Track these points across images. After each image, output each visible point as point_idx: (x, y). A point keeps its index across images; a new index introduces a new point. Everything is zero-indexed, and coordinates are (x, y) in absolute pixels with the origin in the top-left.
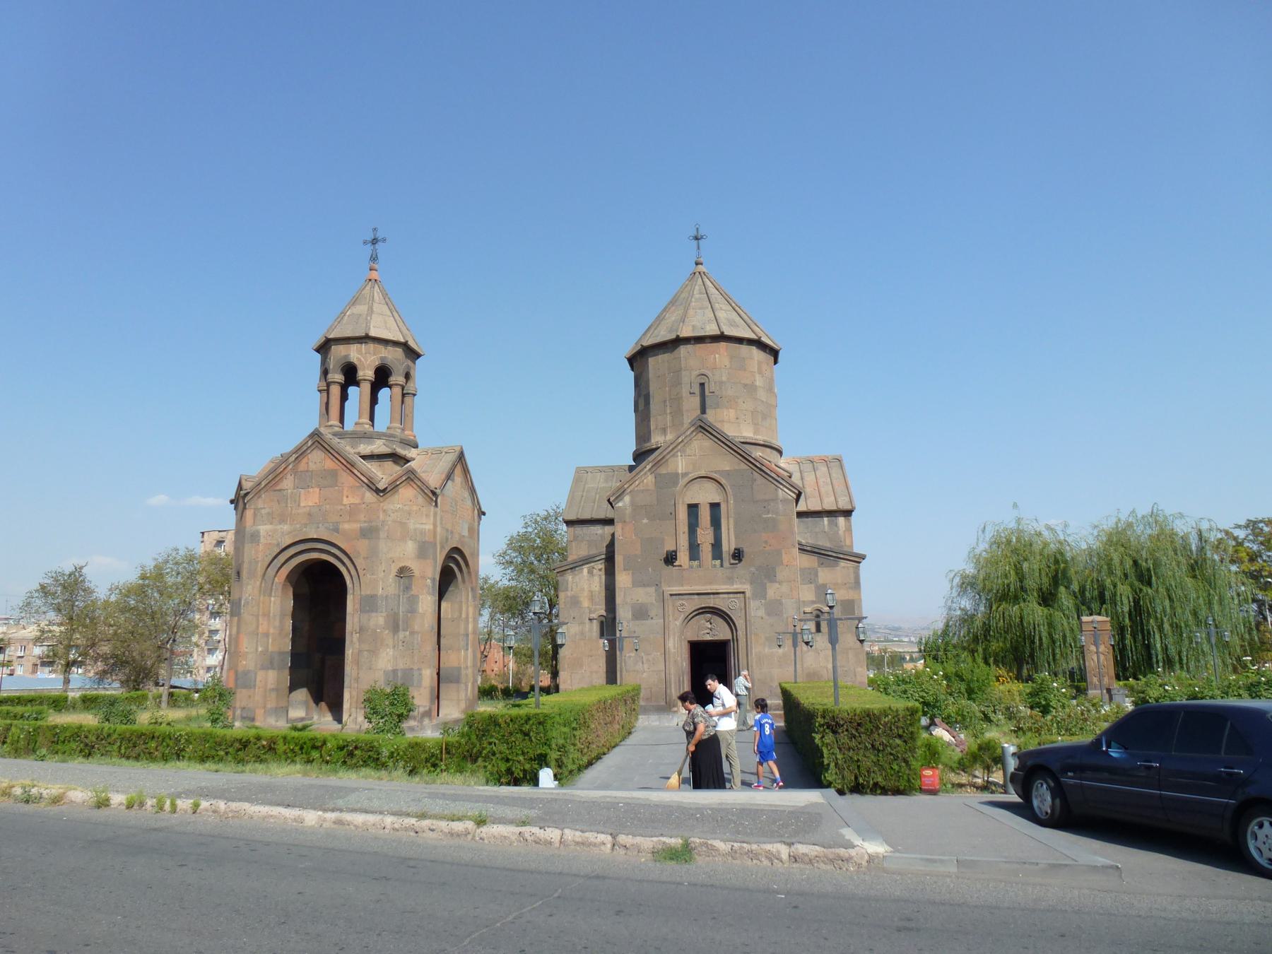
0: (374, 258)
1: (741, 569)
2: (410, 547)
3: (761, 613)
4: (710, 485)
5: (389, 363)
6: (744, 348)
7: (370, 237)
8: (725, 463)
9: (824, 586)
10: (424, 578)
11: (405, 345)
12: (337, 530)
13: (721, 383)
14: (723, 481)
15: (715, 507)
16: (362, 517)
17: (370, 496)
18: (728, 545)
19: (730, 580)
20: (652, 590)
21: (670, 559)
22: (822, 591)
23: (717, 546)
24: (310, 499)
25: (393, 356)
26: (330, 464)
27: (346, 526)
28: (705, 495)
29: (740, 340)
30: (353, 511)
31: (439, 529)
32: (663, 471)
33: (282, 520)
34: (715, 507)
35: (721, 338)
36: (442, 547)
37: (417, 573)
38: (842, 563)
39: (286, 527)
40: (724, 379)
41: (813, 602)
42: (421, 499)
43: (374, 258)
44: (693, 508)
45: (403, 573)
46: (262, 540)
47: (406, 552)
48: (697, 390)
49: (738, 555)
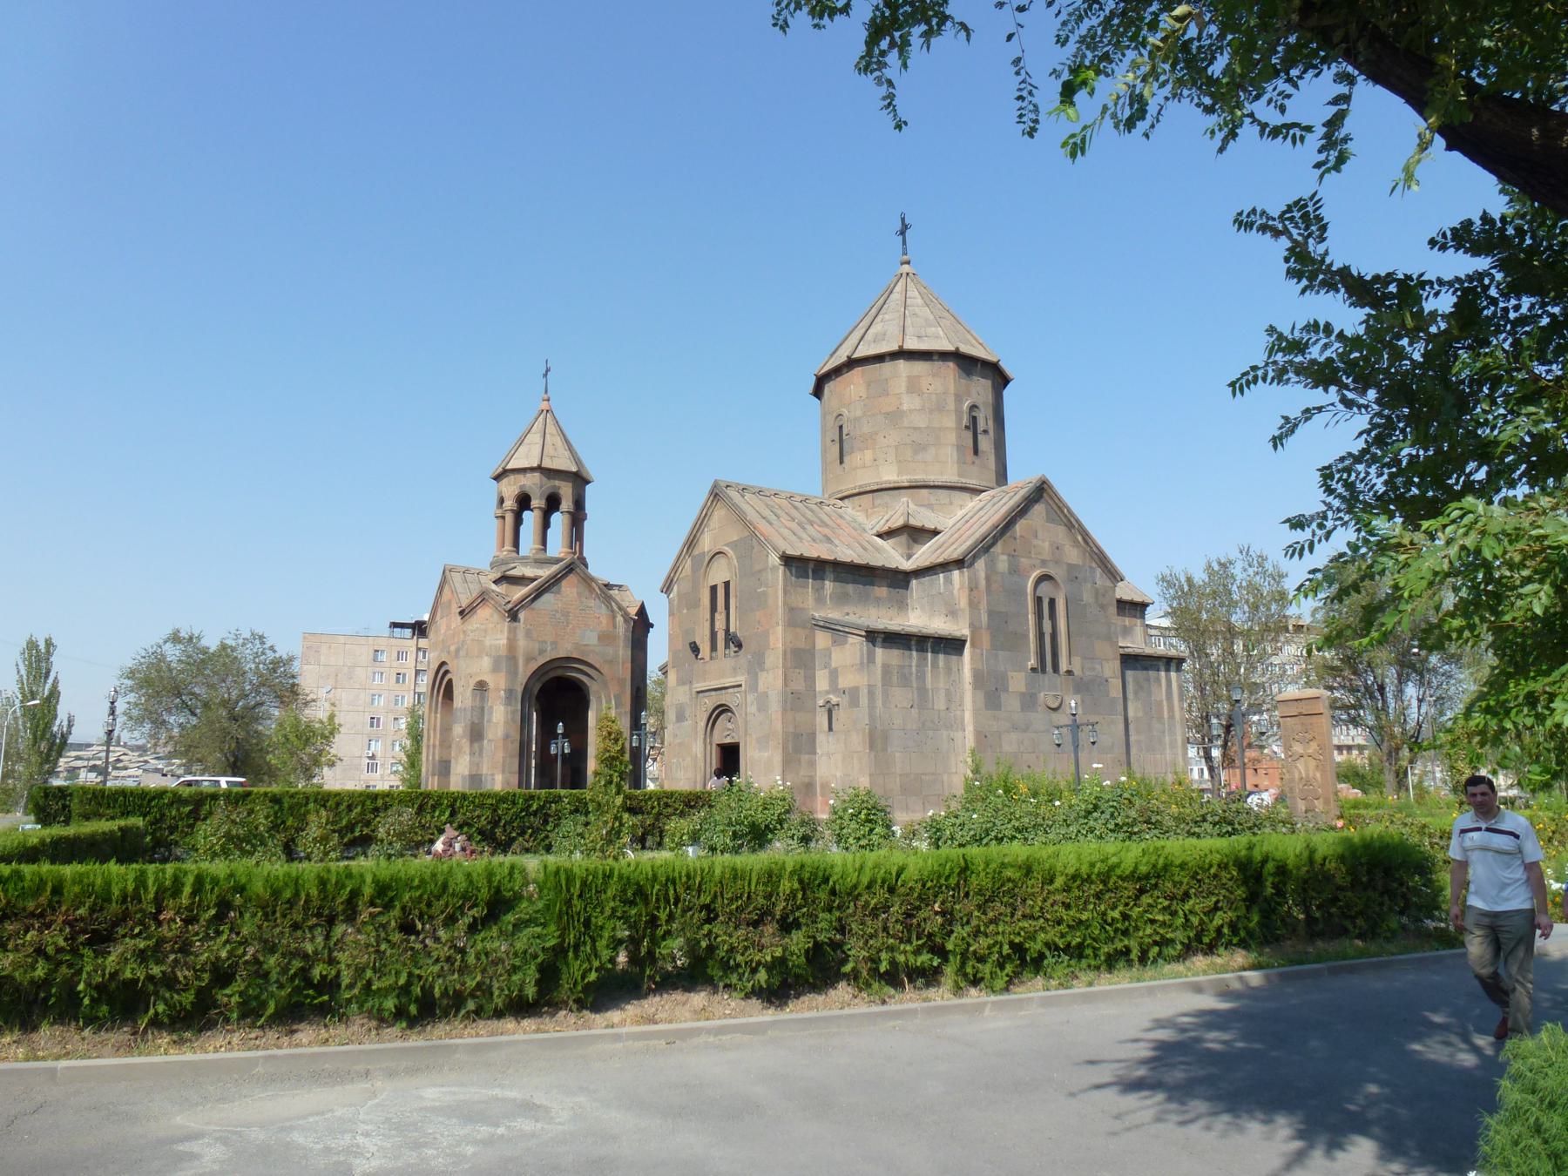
1: (744, 657)
2: (486, 662)
3: (752, 709)
5: (527, 490)
6: (887, 367)
9: (836, 670)
10: (498, 690)
11: (539, 469)
13: (857, 419)
14: (731, 553)
19: (735, 671)
20: (687, 688)
21: (695, 649)
22: (834, 675)
23: (727, 630)
25: (531, 482)
28: (719, 574)
29: (880, 358)
31: (522, 643)
32: (696, 552)
34: (727, 584)
35: (852, 363)
36: (529, 659)
37: (491, 685)
38: (852, 639)
40: (859, 413)
41: (828, 692)
42: (496, 617)
44: (714, 589)
45: (481, 686)
47: (481, 668)
48: (837, 438)
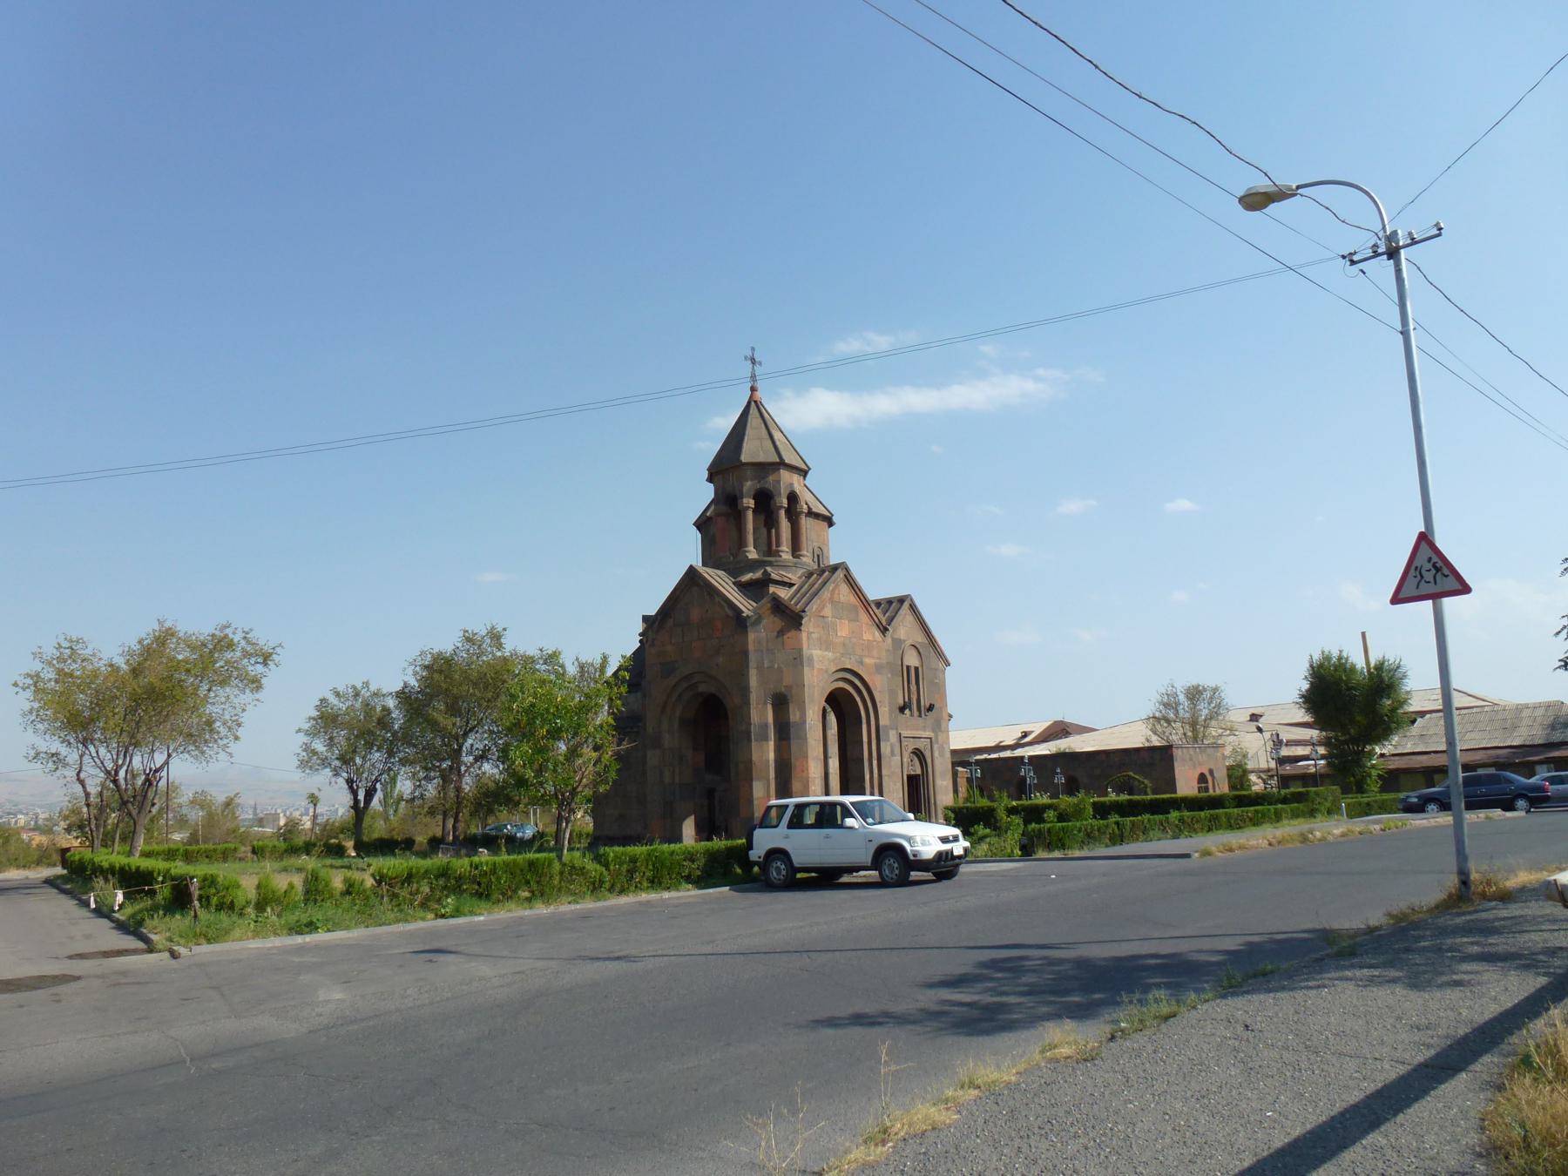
0: (753, 377)
4: (914, 652)
7: (749, 354)
8: (919, 638)
12: (861, 663)
15: (916, 669)
16: (875, 653)
17: (877, 634)
18: (925, 703)
19: (924, 729)
24: (843, 630)
26: (853, 599)
27: (867, 660)
28: (912, 660)
30: (869, 646)
33: (827, 649)
39: (830, 655)
43: (753, 377)
46: (817, 666)
49: (931, 708)
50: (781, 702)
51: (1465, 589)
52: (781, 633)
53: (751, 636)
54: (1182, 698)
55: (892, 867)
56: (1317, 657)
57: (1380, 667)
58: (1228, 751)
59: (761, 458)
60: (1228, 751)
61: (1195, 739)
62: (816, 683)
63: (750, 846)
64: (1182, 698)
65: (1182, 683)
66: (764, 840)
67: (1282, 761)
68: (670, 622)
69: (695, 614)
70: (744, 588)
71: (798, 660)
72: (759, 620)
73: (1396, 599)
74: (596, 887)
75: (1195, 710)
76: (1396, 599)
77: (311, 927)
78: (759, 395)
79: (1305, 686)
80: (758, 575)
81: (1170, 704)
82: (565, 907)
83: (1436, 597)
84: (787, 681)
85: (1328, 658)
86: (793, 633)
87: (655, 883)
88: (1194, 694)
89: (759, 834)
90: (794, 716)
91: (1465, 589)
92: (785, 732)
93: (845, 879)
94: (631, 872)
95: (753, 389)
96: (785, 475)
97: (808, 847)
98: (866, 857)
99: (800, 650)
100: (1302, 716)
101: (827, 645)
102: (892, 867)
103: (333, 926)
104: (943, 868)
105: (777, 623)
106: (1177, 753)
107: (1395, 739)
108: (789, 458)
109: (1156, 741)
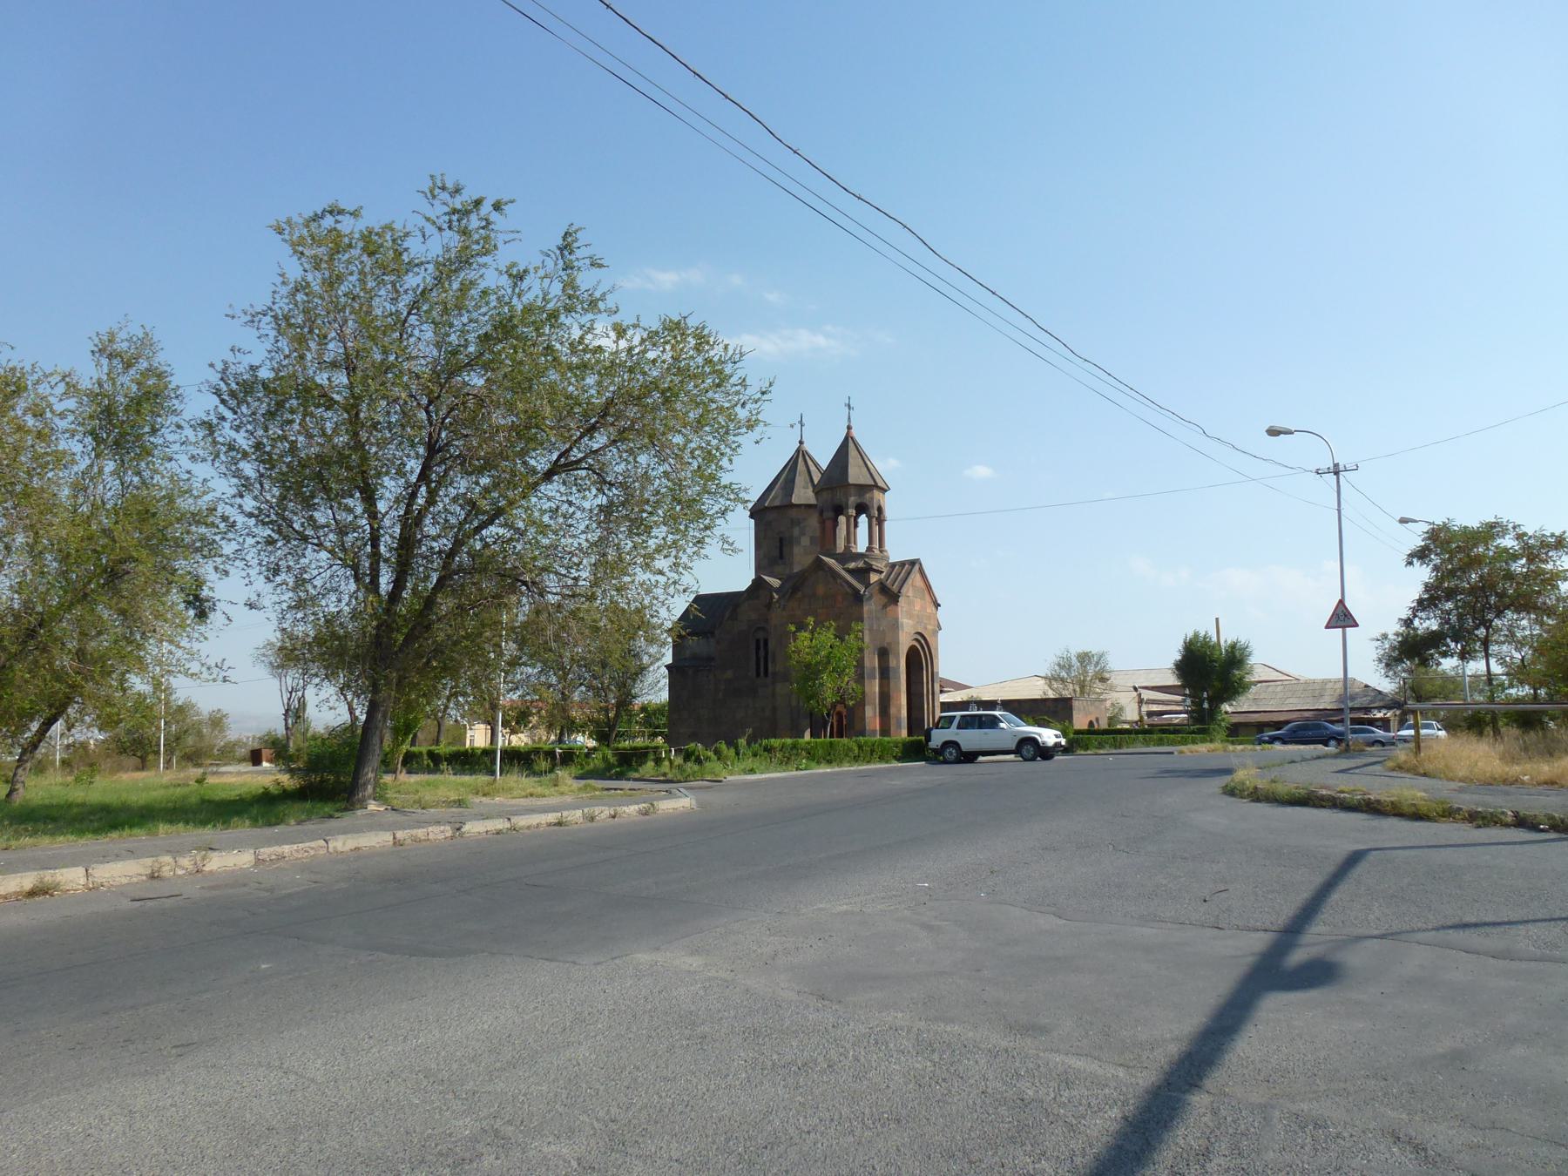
50: (884, 653)
51: (1356, 625)
52: (885, 607)
53: (866, 608)
54: (1074, 660)
55: (1028, 750)
56: (1190, 635)
57: (1233, 646)
58: (1108, 704)
59: (862, 481)
60: (1108, 704)
61: (1082, 692)
62: (905, 642)
63: (928, 739)
64: (1074, 659)
65: (1076, 649)
66: (938, 737)
67: (1150, 714)
68: (799, 594)
69: (821, 590)
70: (849, 571)
71: (895, 626)
72: (871, 597)
73: (1327, 627)
74: (856, 759)
75: (1087, 671)
76: (1327, 627)
77: (752, 771)
78: (854, 433)
79: (1179, 657)
80: (861, 564)
81: (1065, 665)
82: (846, 768)
83: (1344, 627)
84: (888, 640)
85: (1196, 635)
86: (891, 608)
87: (881, 759)
88: (1084, 658)
89: (935, 733)
90: (892, 663)
91: (1356, 625)
92: (885, 673)
93: (981, 758)
94: (872, 751)
95: (849, 428)
96: (876, 493)
97: (970, 739)
98: (1013, 746)
99: (897, 620)
100: (1172, 680)
101: (910, 617)
102: (1028, 750)
103: (767, 770)
104: (1045, 753)
105: (884, 600)
106: (1075, 704)
107: (1242, 698)
108: (881, 484)
109: (1051, 695)
